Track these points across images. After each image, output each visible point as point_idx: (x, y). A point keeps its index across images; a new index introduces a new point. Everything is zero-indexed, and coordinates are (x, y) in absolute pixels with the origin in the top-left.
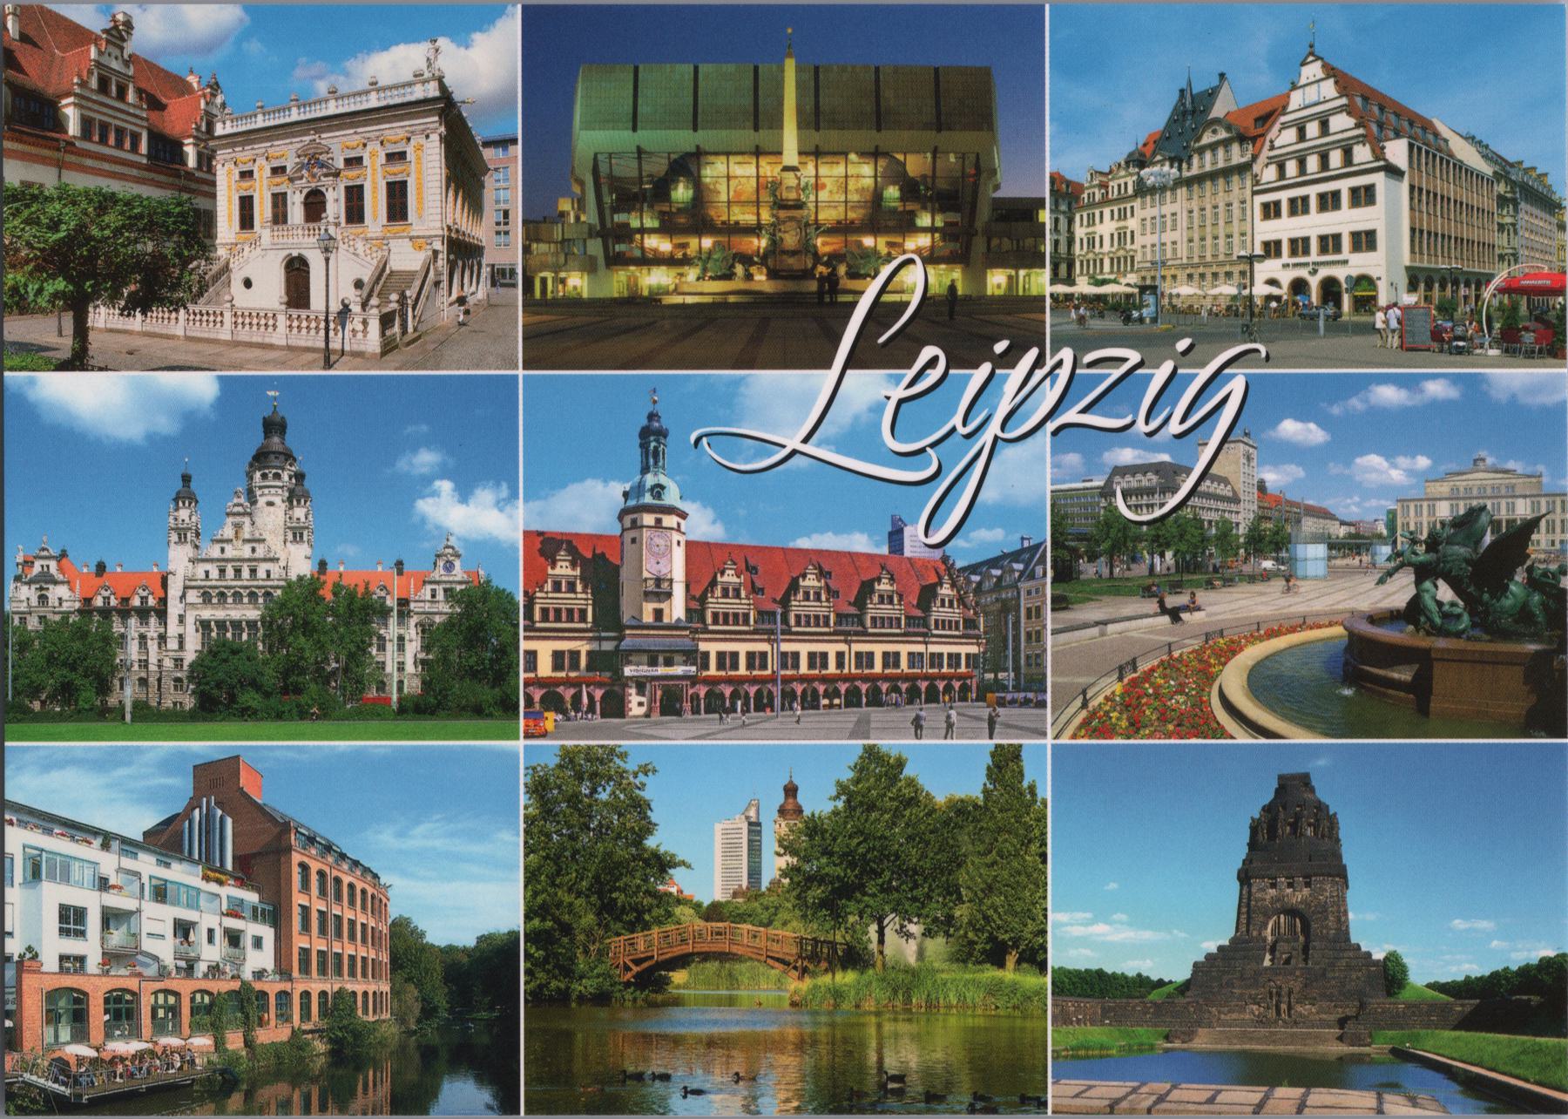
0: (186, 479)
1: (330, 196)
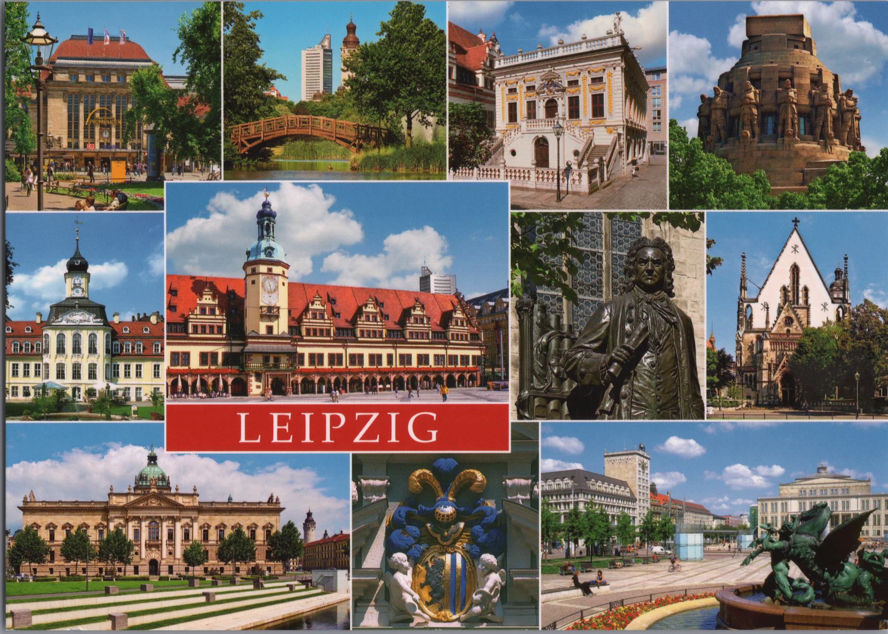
1: (560, 102)
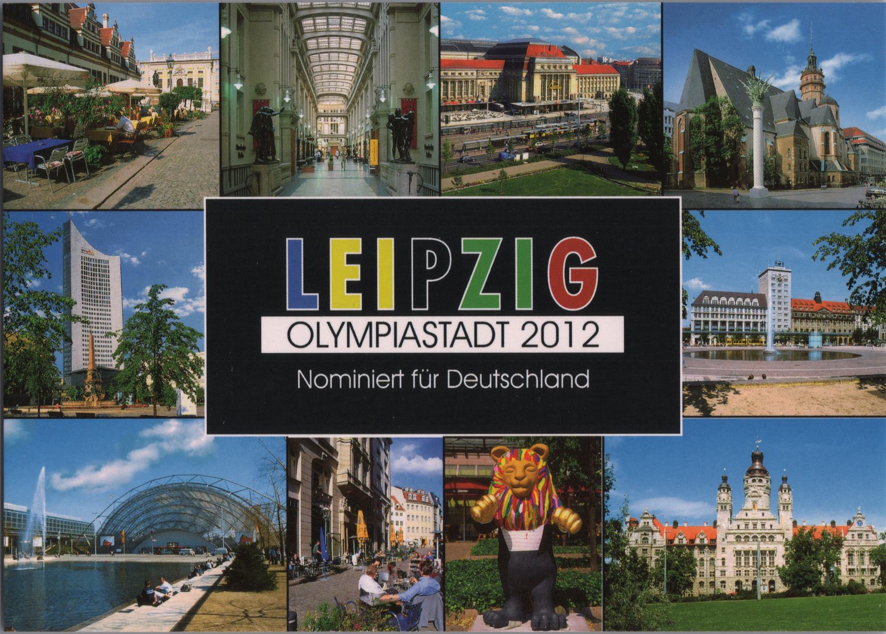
0: (725, 479)
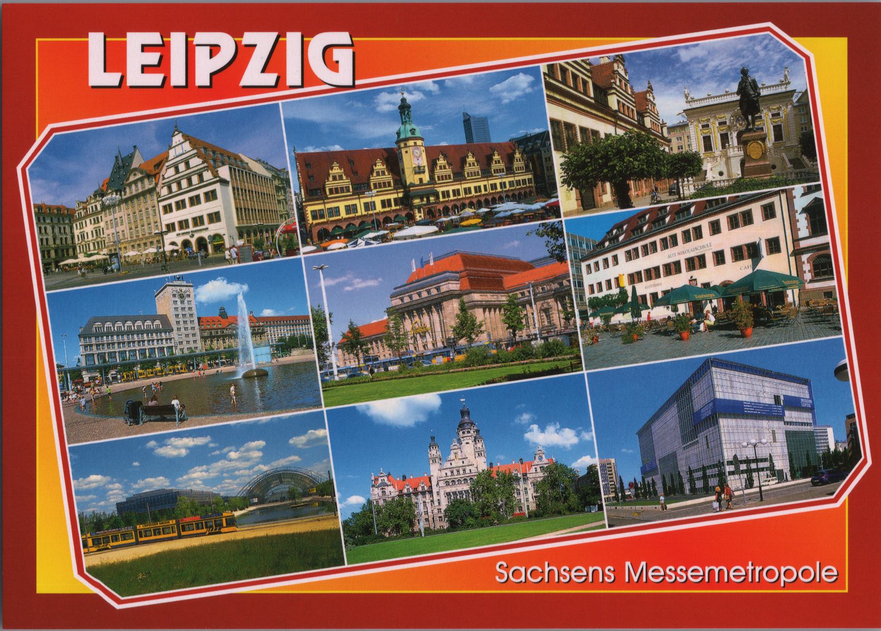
0: (433, 438)
